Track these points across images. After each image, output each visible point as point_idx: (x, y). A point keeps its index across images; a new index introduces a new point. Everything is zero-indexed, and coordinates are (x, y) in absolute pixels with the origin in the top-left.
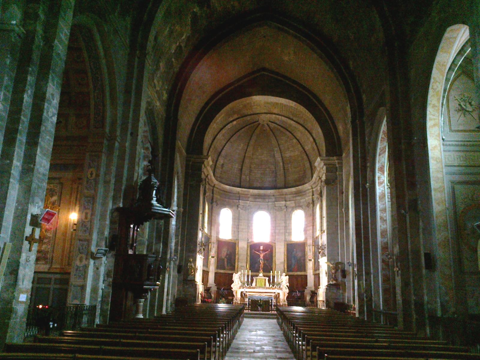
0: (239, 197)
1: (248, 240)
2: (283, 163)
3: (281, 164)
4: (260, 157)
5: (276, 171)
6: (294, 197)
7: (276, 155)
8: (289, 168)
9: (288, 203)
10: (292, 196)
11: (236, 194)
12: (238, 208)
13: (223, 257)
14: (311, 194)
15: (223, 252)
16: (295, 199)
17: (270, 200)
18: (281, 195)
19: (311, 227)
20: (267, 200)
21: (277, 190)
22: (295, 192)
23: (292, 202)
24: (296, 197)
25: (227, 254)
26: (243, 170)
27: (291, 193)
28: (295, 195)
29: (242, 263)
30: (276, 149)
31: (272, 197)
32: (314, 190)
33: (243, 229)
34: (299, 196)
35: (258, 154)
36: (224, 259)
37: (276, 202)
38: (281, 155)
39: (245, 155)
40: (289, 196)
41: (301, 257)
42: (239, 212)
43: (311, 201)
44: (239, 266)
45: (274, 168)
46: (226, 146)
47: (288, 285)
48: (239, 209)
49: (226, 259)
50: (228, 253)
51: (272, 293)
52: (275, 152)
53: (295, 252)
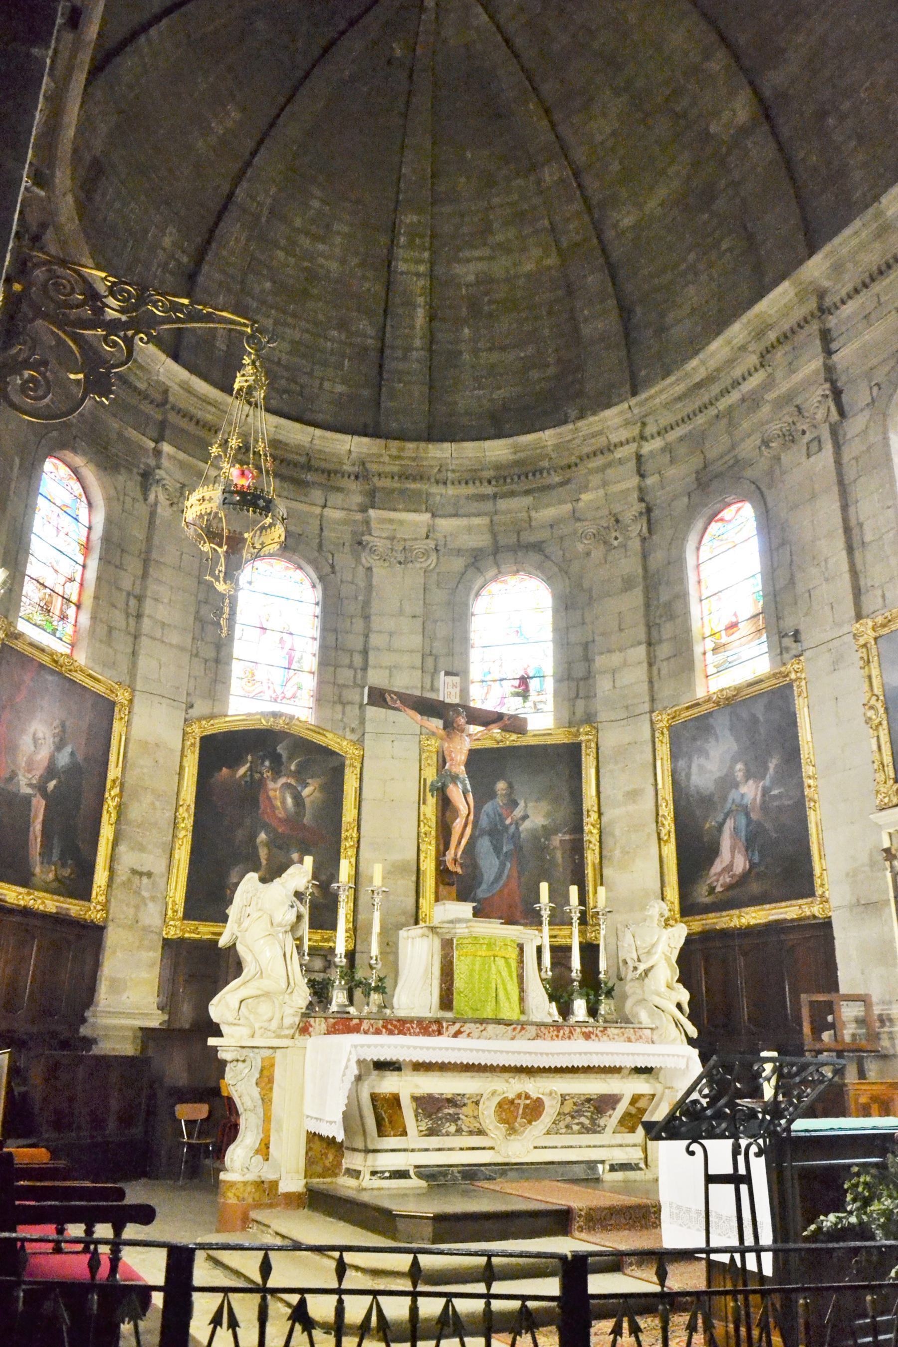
0: (162, 425)
1: (192, 706)
2: (432, 318)
3: (420, 317)
4: (305, 242)
5: (382, 351)
6: (482, 498)
7: (400, 253)
8: (463, 347)
9: (445, 525)
10: (471, 490)
11: (144, 396)
12: (145, 491)
13: (24, 785)
14: (632, 464)
15: (26, 743)
16: (488, 506)
17: (336, 498)
18: (404, 476)
19: (641, 651)
20: (317, 495)
21: (394, 444)
22: (498, 467)
23: (476, 521)
24: (495, 496)
25: (51, 771)
26: (201, 279)
27: (471, 476)
28: (489, 490)
29: (142, 848)
30: (410, 218)
31: (353, 485)
32: (647, 448)
33: (163, 625)
34: (512, 494)
35: (298, 222)
36: (27, 800)
37: (372, 512)
38: (432, 263)
39: (231, 195)
40: (451, 491)
41: (548, 831)
42: (153, 514)
43: (631, 509)
44: (122, 874)
45: (371, 331)
46: (153, 32)
47: (684, 996)
48: (157, 494)
49: (39, 806)
50: (63, 759)
51: (614, 1070)
52: (402, 239)
53: (500, 801)
